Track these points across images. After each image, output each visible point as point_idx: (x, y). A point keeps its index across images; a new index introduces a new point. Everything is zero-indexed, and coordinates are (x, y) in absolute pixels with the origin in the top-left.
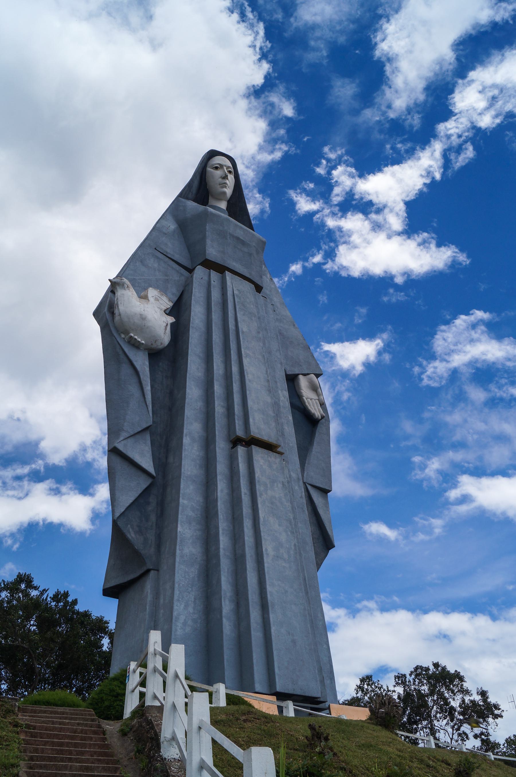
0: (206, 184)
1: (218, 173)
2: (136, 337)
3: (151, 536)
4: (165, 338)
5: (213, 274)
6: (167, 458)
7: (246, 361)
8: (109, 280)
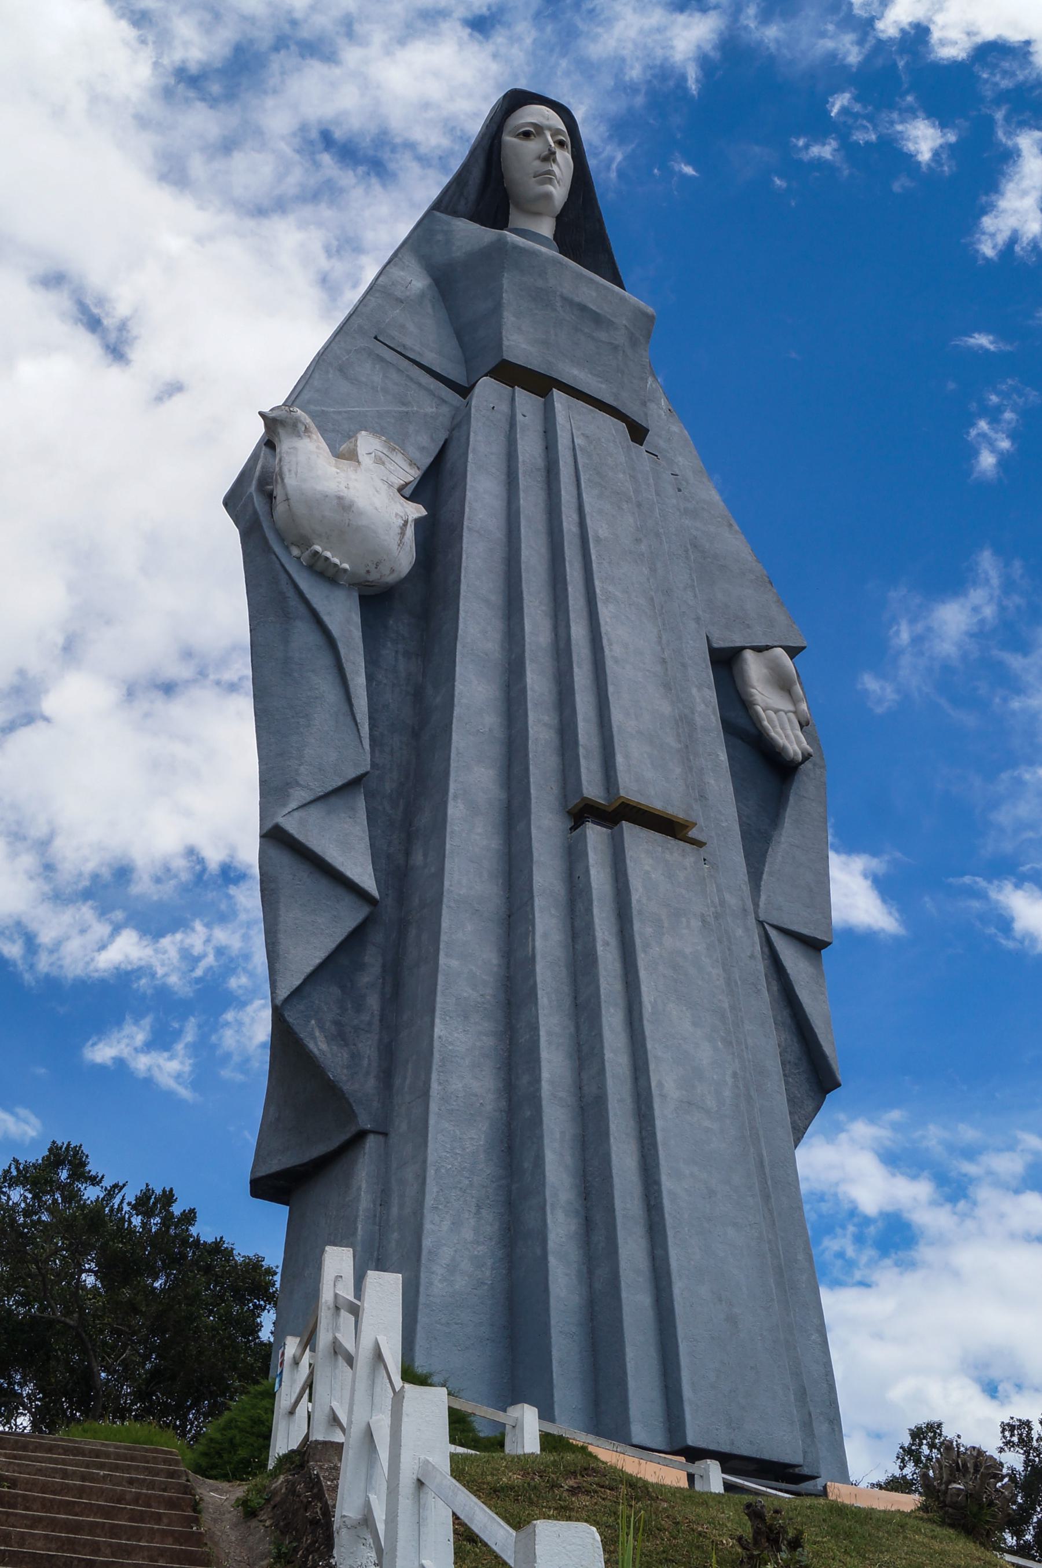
0: (501, 177)
1: (533, 147)
2: (328, 554)
3: (368, 1047)
4: (402, 557)
5: (521, 395)
6: (408, 853)
7: (605, 612)
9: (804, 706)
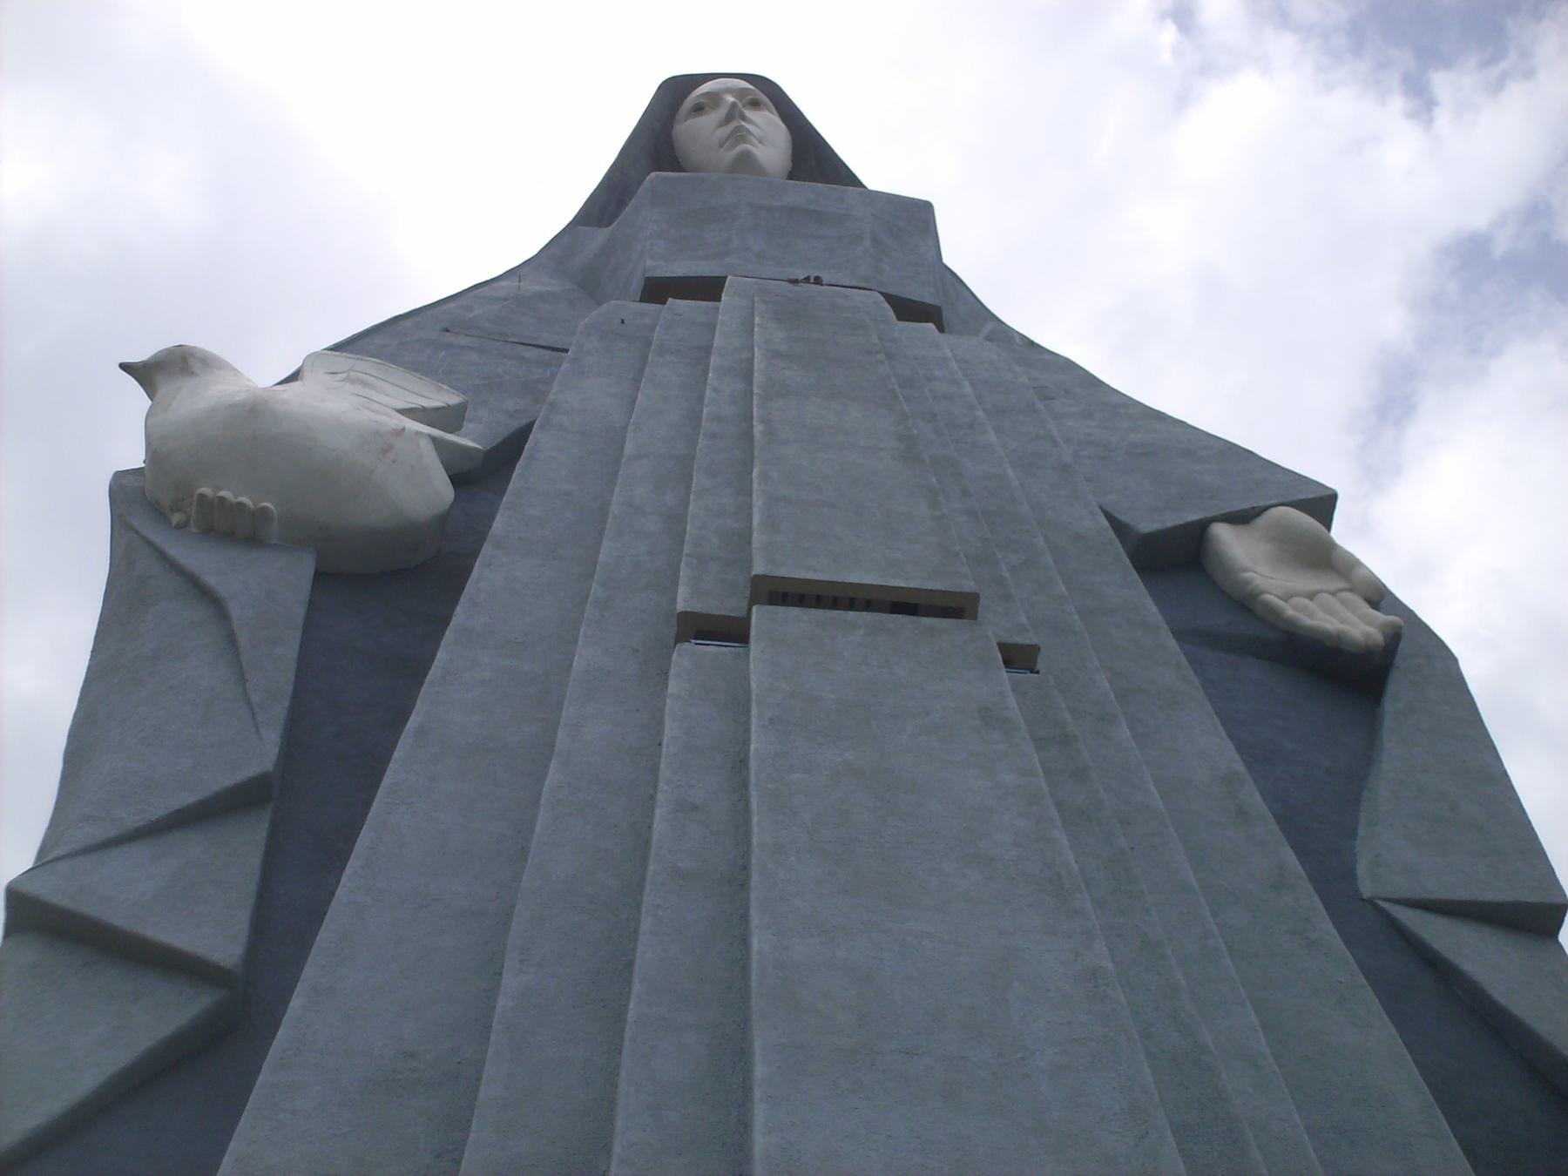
1: (710, 119)
2: (222, 493)
8: (125, 367)
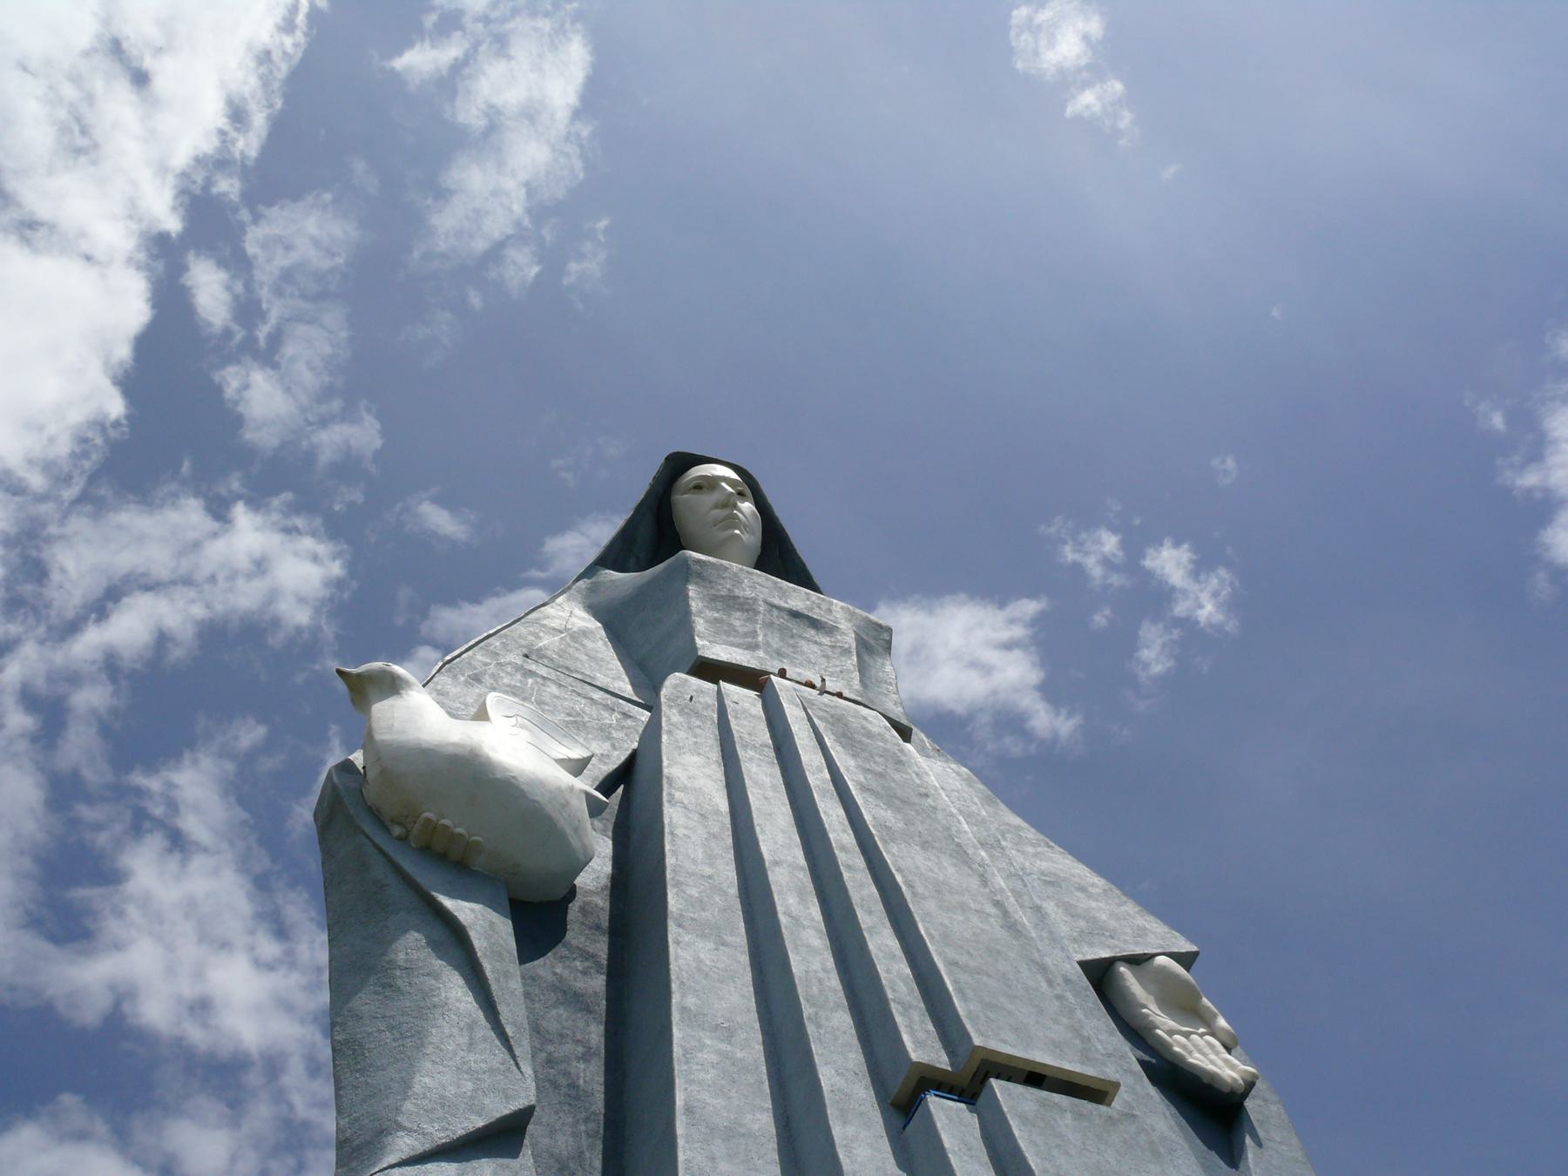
9: (1222, 1022)
